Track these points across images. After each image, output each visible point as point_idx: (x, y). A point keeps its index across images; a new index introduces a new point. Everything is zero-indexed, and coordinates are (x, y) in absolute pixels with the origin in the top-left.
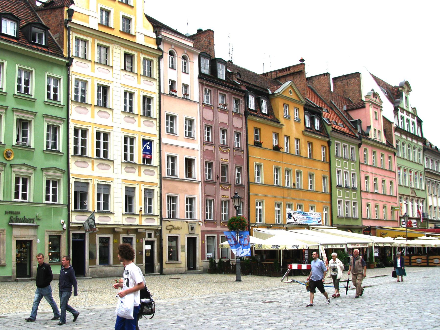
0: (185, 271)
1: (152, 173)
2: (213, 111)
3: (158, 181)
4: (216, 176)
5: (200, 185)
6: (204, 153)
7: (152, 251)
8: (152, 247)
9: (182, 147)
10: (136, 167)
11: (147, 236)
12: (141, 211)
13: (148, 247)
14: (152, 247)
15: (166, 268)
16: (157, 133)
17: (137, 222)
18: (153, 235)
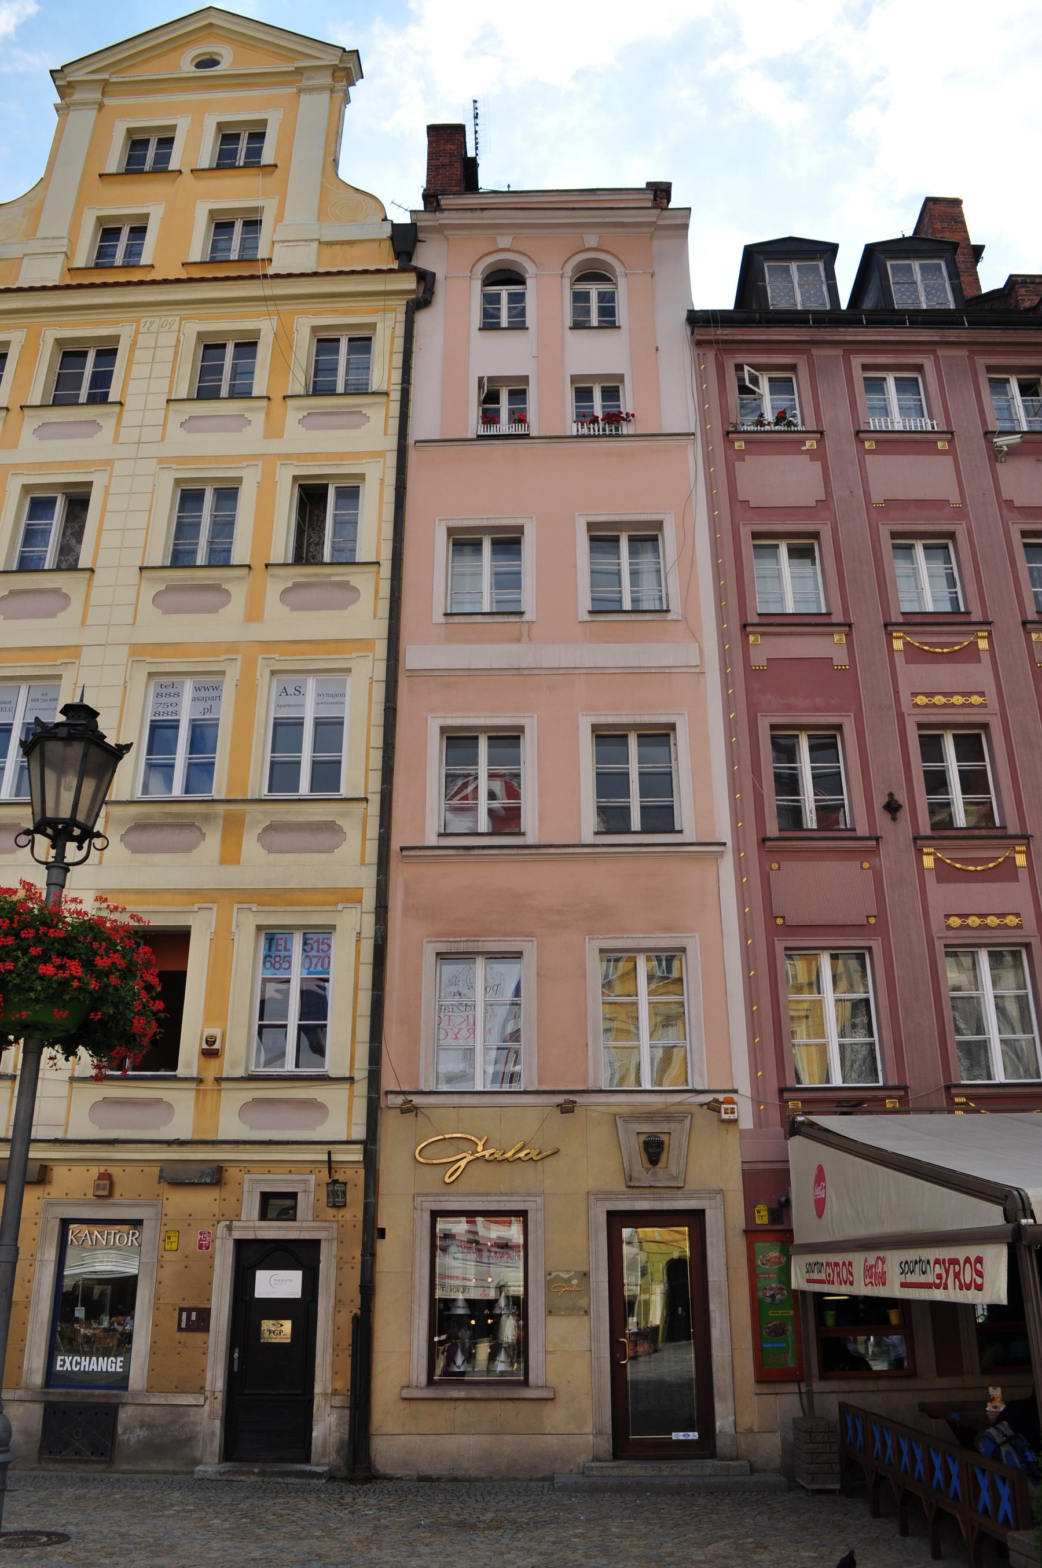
0: (583, 1459)
1: (321, 838)
2: (819, 455)
3: (368, 878)
4: (880, 800)
5: (727, 866)
6: (752, 685)
7: (302, 1311)
8: (310, 1285)
9: (569, 672)
10: (207, 818)
11: (252, 1207)
12: (210, 1053)
13: (277, 1284)
14: (310, 1285)
15: (402, 1434)
16: (380, 629)
17: (181, 1126)
18: (304, 1206)
